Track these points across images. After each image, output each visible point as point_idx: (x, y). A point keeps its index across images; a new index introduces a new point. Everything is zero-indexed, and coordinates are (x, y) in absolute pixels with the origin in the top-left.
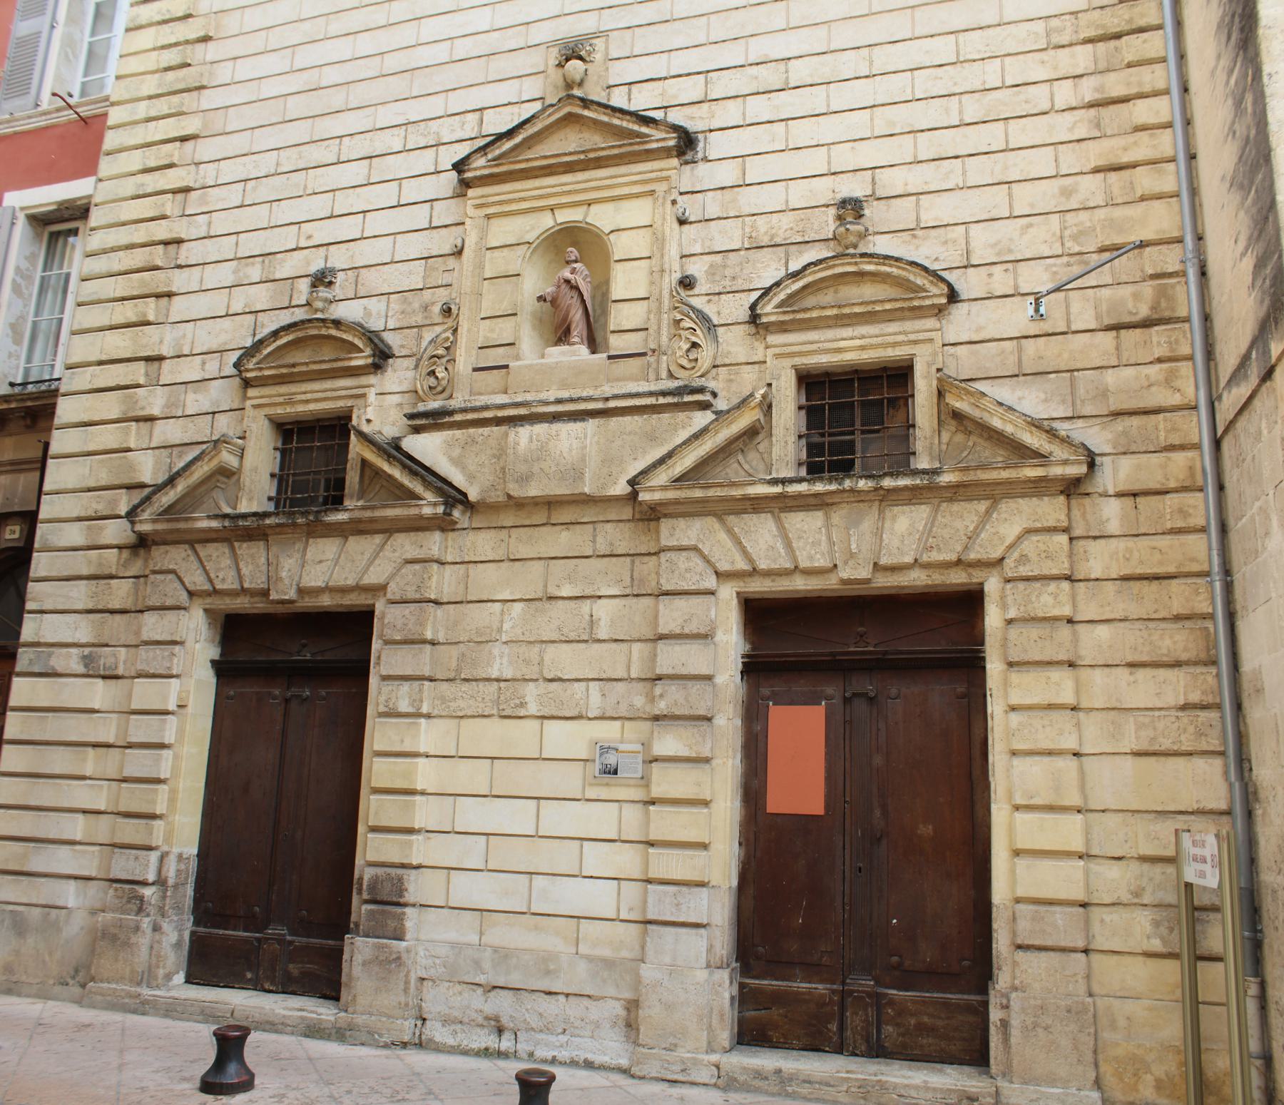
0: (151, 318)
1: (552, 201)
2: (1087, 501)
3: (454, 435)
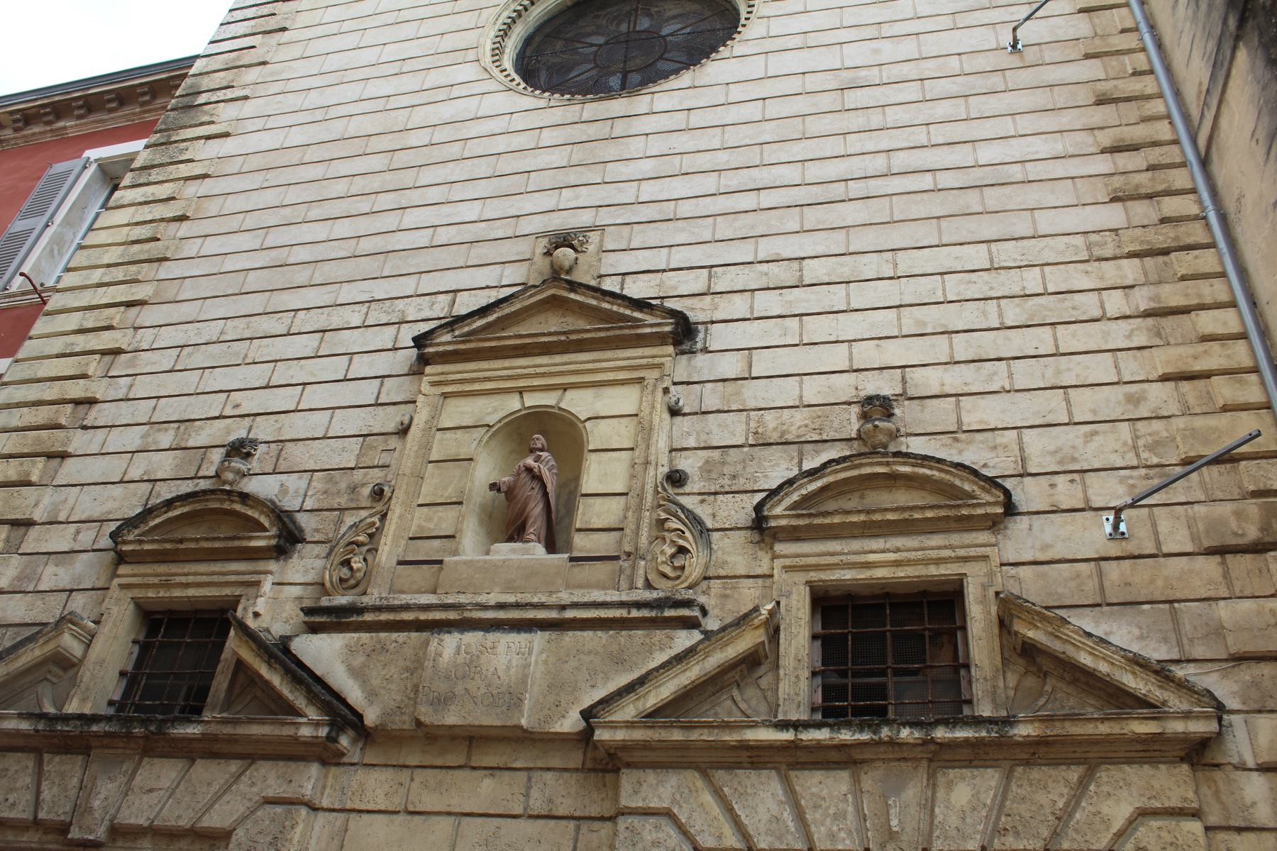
0: (34, 478)
1: (521, 383)
3: (359, 639)
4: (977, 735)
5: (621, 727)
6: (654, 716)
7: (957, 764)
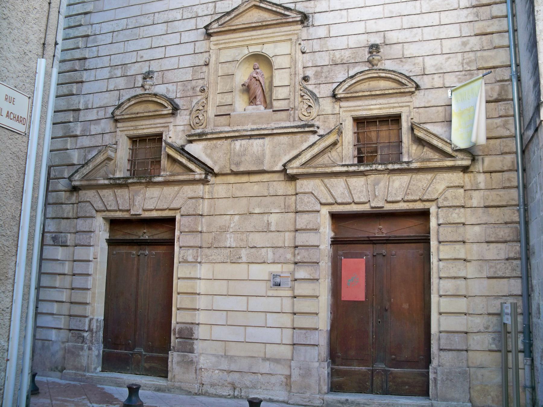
0: (75, 92)
1: (247, 43)
3: (207, 144)
6: (303, 165)
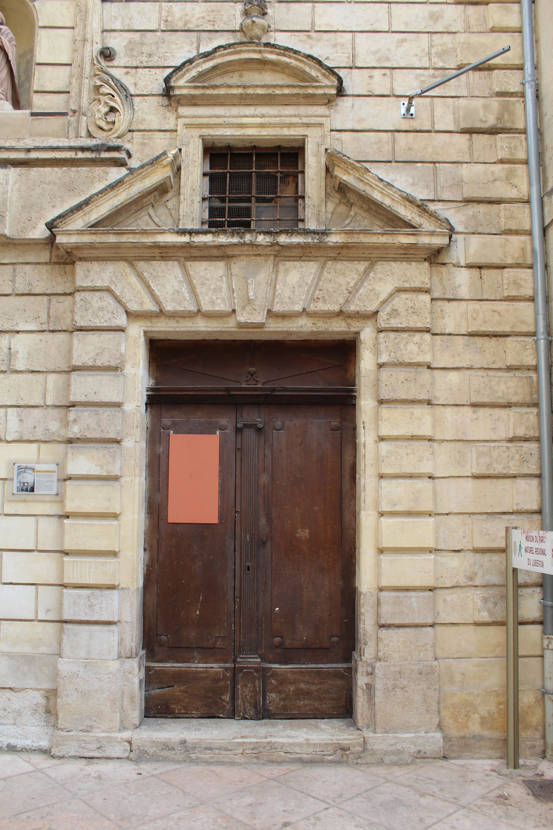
2: (444, 269)
4: (305, 241)
5: (74, 234)
7: (292, 259)
